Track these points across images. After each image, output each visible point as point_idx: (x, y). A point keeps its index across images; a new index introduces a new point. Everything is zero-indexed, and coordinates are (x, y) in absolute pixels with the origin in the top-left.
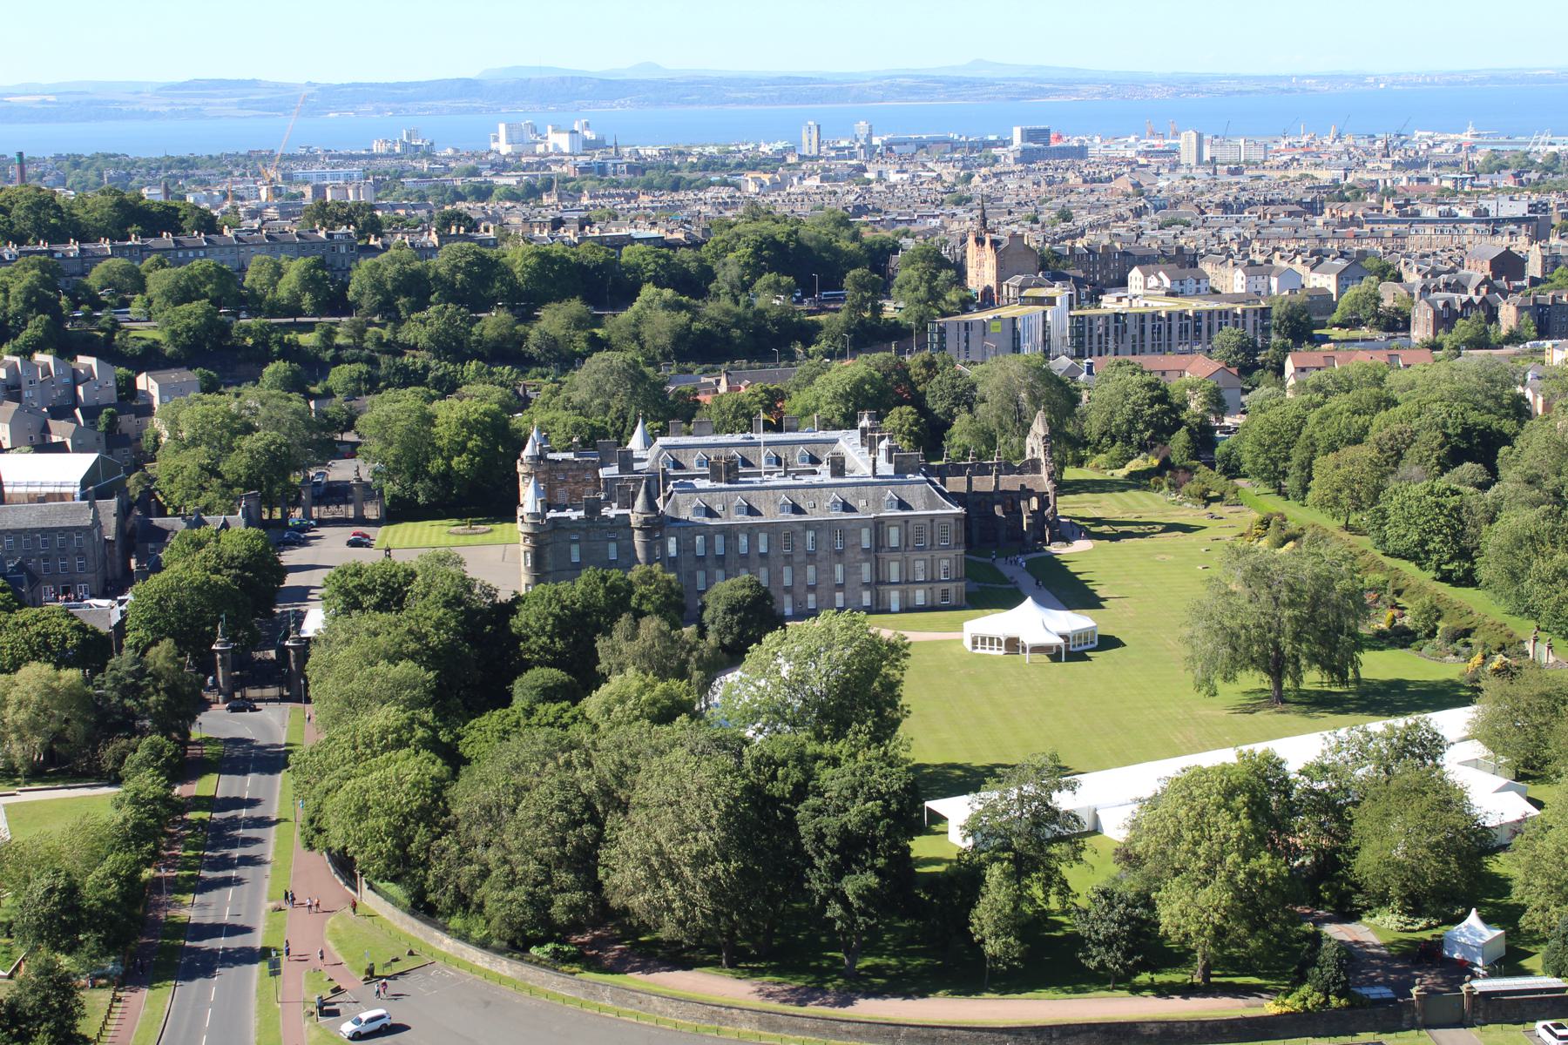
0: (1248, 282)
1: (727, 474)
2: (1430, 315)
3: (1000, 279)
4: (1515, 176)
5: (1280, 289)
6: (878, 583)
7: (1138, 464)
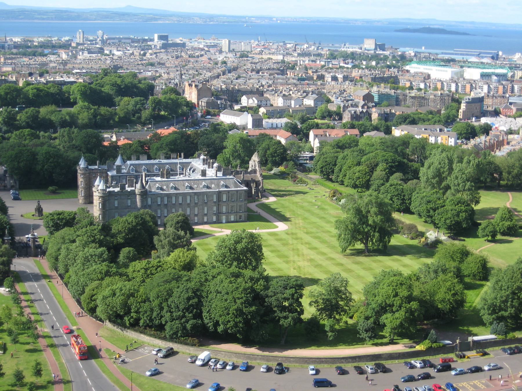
0: (284, 102)
1: (166, 175)
2: (350, 116)
3: (198, 99)
4: (344, 60)
5: (295, 105)
6: (219, 213)
7: (275, 170)
